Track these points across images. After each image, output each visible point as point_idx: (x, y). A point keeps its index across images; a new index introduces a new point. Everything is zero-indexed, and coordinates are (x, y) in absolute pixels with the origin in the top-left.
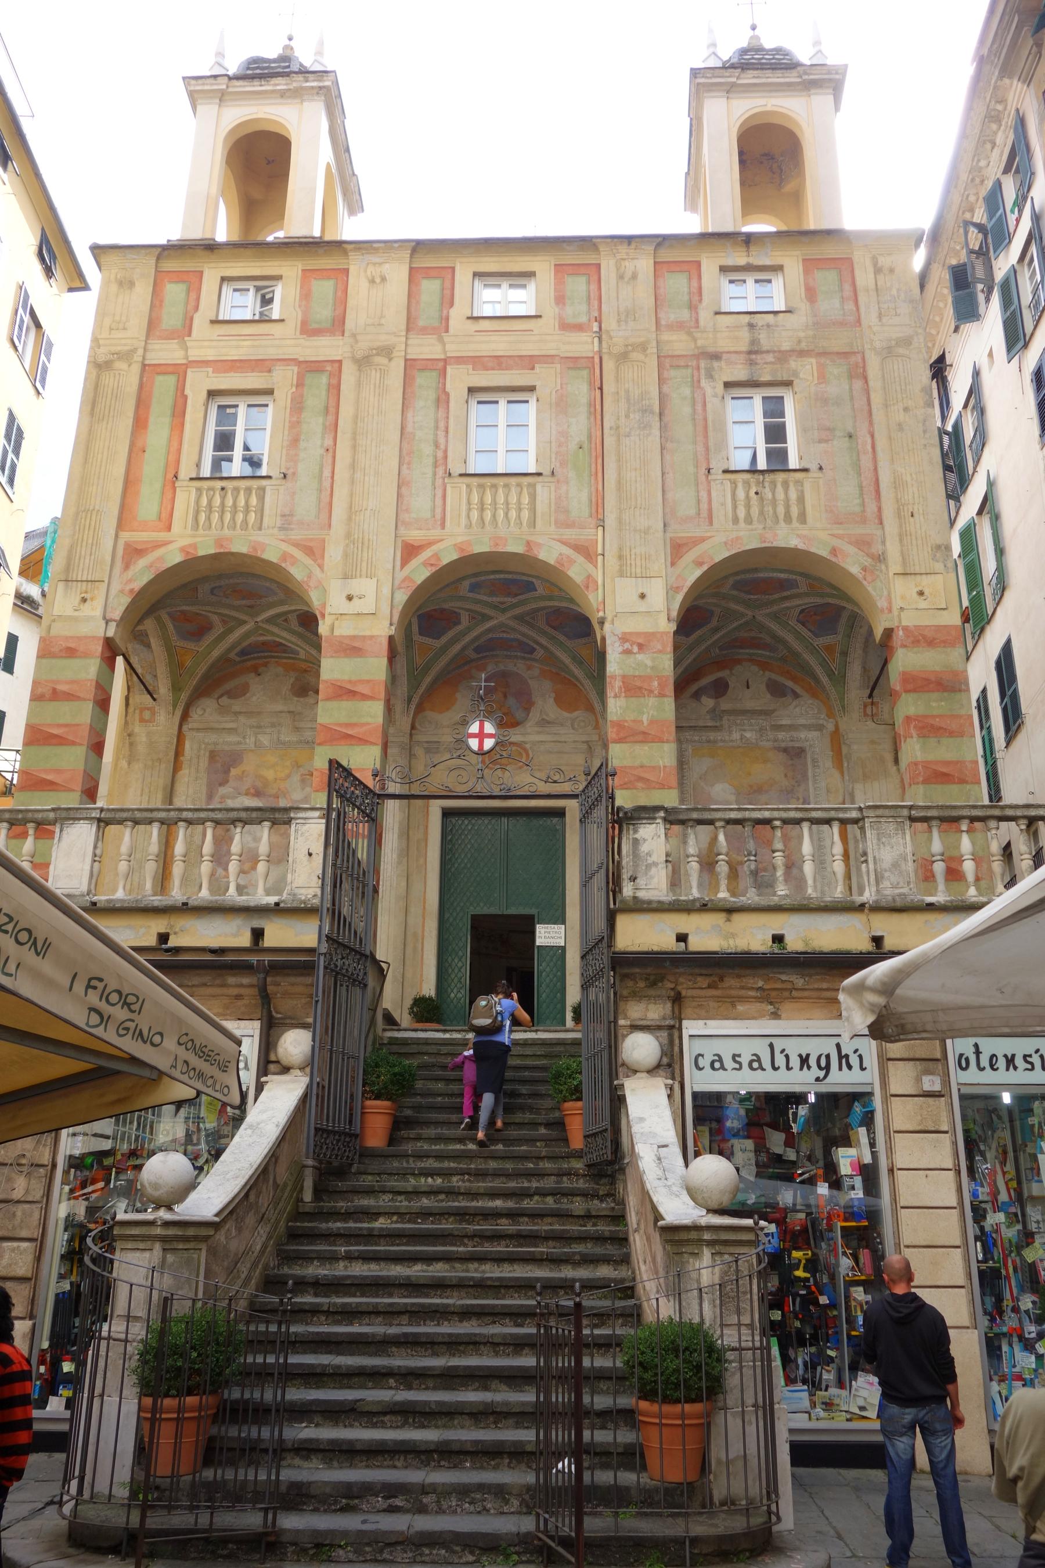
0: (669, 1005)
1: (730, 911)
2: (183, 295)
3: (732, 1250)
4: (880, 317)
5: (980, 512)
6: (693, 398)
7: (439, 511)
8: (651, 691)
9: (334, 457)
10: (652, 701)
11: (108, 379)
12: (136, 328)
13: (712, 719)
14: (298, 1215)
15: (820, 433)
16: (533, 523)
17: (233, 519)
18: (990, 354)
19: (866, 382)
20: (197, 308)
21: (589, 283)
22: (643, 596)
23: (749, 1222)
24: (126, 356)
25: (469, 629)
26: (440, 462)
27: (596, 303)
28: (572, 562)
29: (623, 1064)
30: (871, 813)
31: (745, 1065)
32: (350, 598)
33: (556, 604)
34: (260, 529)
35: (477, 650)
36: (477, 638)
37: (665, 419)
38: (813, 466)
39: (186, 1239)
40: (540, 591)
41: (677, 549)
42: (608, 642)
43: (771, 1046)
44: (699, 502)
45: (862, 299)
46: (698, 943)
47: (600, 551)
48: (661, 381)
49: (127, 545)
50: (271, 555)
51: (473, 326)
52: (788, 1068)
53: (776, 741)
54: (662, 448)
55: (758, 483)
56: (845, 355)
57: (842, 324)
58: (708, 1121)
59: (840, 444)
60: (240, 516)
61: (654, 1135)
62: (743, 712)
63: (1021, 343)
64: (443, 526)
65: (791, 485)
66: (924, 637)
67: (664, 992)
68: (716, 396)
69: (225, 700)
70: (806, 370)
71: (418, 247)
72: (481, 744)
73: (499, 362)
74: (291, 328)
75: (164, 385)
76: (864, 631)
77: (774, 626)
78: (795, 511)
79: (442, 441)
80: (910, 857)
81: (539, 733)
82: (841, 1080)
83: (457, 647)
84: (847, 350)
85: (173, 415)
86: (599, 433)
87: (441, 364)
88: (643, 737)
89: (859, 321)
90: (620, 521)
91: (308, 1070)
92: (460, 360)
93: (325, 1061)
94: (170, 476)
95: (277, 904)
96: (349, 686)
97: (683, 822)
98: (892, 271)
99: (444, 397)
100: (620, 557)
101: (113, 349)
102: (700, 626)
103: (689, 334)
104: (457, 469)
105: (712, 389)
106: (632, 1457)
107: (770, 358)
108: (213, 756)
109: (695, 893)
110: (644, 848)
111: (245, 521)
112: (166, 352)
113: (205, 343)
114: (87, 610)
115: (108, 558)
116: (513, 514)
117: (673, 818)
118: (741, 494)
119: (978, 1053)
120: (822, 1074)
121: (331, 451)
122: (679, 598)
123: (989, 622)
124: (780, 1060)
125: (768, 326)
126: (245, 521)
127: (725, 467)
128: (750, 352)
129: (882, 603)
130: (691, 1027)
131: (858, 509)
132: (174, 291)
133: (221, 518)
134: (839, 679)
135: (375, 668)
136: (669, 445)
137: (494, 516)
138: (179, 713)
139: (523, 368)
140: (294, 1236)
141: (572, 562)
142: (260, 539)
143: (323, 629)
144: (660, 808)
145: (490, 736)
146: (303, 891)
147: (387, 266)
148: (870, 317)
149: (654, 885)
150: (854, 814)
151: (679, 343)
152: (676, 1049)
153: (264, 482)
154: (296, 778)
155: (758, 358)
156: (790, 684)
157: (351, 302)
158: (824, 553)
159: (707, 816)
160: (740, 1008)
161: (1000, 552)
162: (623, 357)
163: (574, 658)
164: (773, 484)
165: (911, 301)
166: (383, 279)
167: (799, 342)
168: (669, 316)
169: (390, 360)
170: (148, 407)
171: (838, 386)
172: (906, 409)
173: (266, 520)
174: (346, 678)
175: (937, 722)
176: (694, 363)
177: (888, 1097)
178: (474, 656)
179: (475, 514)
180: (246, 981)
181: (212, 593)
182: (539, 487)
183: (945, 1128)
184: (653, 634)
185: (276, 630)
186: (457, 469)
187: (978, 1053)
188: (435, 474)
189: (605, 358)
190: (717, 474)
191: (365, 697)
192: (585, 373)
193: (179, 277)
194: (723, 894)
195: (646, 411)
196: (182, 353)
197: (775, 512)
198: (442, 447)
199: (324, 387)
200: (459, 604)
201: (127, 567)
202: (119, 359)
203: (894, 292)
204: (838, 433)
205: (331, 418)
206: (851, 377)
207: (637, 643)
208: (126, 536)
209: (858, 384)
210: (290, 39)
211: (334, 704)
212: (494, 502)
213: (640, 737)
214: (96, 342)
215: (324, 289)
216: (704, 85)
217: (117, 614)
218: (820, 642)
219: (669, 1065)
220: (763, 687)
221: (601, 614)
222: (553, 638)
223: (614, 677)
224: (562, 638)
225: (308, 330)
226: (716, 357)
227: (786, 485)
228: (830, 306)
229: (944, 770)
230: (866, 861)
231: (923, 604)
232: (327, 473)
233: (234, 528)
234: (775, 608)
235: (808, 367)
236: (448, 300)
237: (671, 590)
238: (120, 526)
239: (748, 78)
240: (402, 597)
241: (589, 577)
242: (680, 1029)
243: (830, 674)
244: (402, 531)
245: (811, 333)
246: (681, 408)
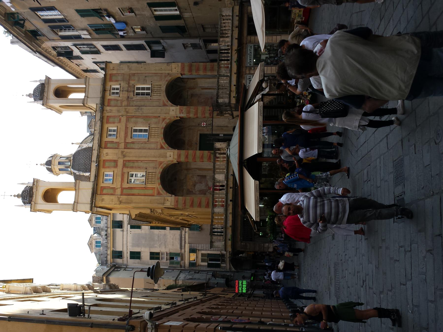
10: (191, 110)
11: (124, 201)
15: (145, 82)
16: (158, 128)
24: (119, 198)
41: (165, 105)
48: (132, 106)
50: (161, 170)
56: (130, 76)
59: (147, 78)
70: (132, 82)
74: (116, 170)
90: (159, 114)
92: (125, 140)
104: (147, 140)
107: (129, 88)
112: (119, 192)
113: (117, 185)
114: (170, 200)
121: (141, 161)
135: (183, 152)
143: (175, 162)
148: (123, 72)
149: (227, 100)
151: (125, 103)
158: (167, 83)
162: (127, 112)
191: (188, 153)
196: (119, 189)
201: (162, 194)
207: (181, 111)
208: (155, 195)
217: (170, 195)
225: (116, 166)
226: (128, 97)
227: (154, 87)
228: (120, 78)
232: (146, 162)
236: (112, 142)
237: (172, 106)
239: (45, 94)
246: (138, 103)
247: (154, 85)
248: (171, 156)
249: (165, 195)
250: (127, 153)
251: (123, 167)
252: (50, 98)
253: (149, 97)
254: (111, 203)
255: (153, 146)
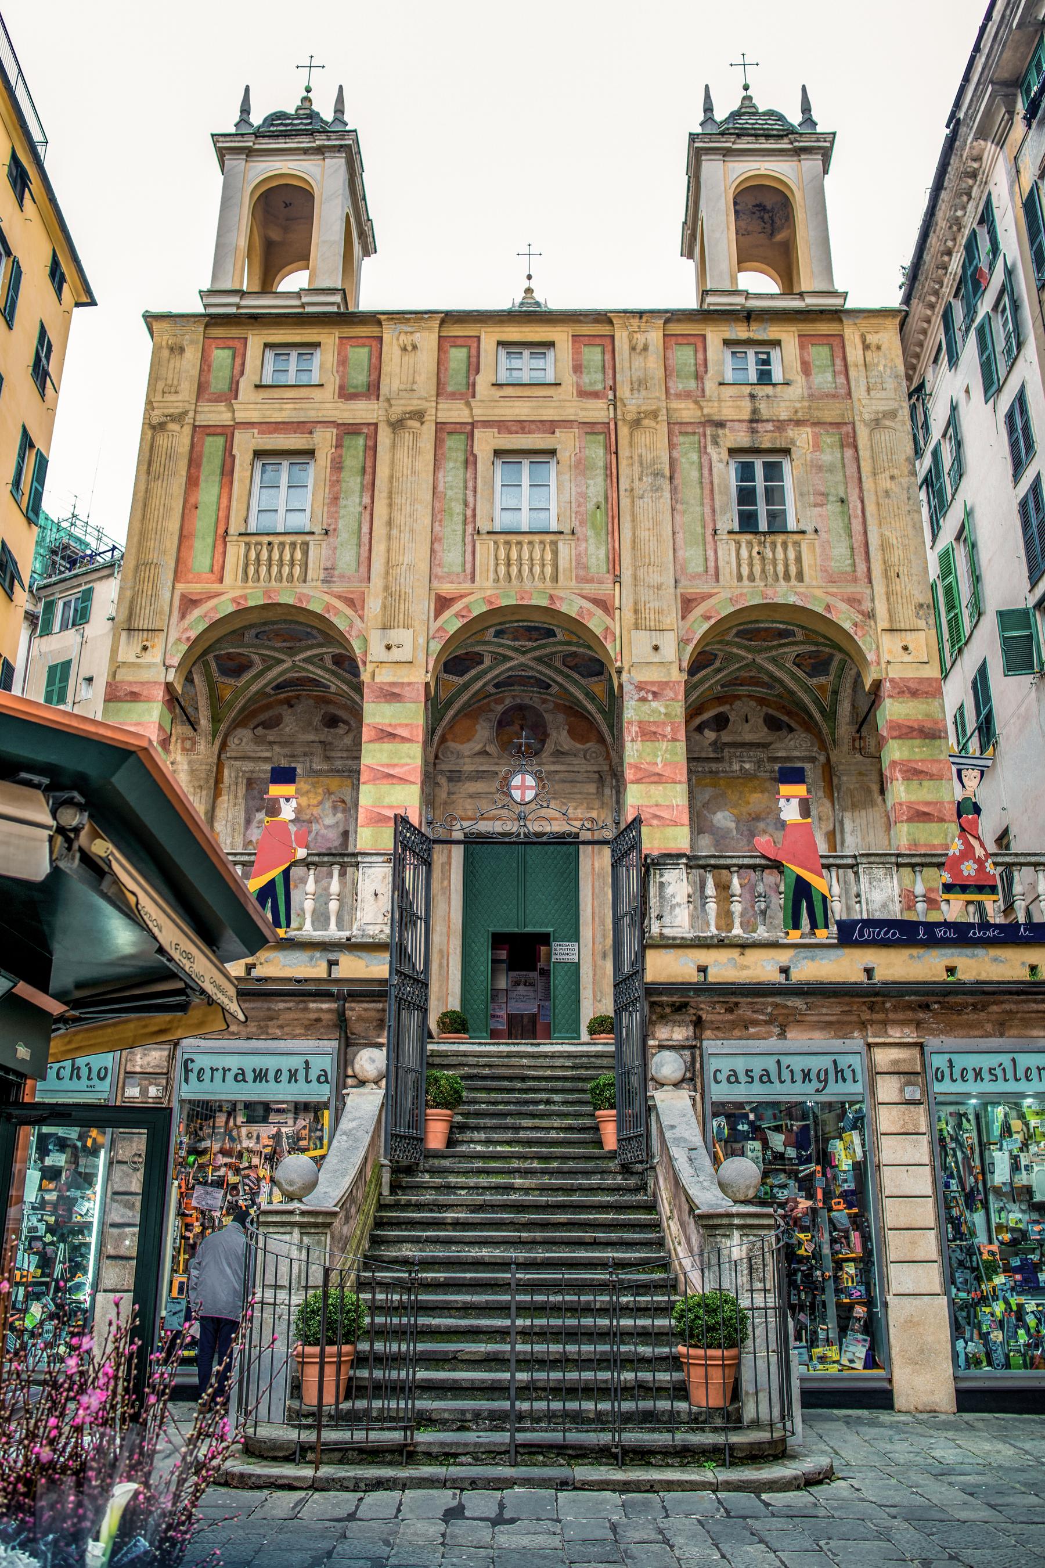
0: (691, 1028)
1: (744, 946)
2: (229, 361)
3: (755, 1232)
4: (868, 390)
5: (958, 539)
6: (701, 463)
7: (469, 566)
8: (665, 736)
9: (372, 515)
10: (664, 745)
11: (162, 440)
12: (187, 391)
13: (714, 751)
14: (382, 1207)
16: (555, 578)
17: (280, 572)
18: (967, 391)
19: (857, 451)
20: (242, 373)
21: (603, 353)
22: (656, 648)
23: (771, 1210)
24: (178, 418)
25: (490, 668)
26: (470, 520)
27: (610, 372)
28: (591, 614)
29: (652, 1079)
30: (864, 860)
31: (756, 1079)
32: (388, 647)
33: (574, 649)
34: (305, 581)
35: (497, 686)
36: (497, 676)
37: (676, 482)
38: (809, 529)
39: (316, 1225)
40: (560, 637)
42: (625, 690)
43: (778, 1062)
44: (706, 560)
45: (852, 373)
46: (714, 975)
47: (617, 605)
48: (671, 446)
49: (183, 596)
51: (498, 393)
52: (793, 1082)
53: (772, 772)
54: (673, 510)
55: (760, 543)
57: (834, 396)
58: (733, 1127)
59: (833, 507)
60: (286, 570)
61: (685, 1140)
62: (743, 745)
63: (995, 388)
64: (473, 580)
65: (790, 545)
66: (908, 688)
67: (688, 1019)
68: (721, 461)
69: (260, 731)
70: (802, 438)
71: (449, 318)
72: (523, 794)
73: (522, 426)
74: (329, 392)
75: (214, 445)
76: (853, 672)
77: (771, 667)
78: (793, 570)
79: (471, 499)
80: (897, 899)
81: (554, 763)
82: (836, 1091)
83: (479, 684)
84: (839, 420)
85: (222, 474)
86: (615, 495)
87: (469, 427)
88: (658, 779)
89: (849, 394)
90: (635, 577)
91: (384, 1083)
92: (487, 424)
93: (393, 1074)
94: (221, 531)
95: (349, 939)
96: (389, 730)
97: (704, 867)
98: (879, 348)
99: (471, 458)
100: (636, 611)
101: (167, 411)
102: (704, 667)
103: (696, 402)
104: (484, 527)
105: (717, 455)
106: (681, 1391)
107: (770, 426)
108: (250, 783)
109: (713, 930)
110: (669, 891)
111: (291, 574)
112: (216, 414)
115: (167, 609)
116: (537, 569)
117: (693, 863)
118: (744, 553)
119: (951, 1066)
120: (821, 1086)
121: (370, 509)
122: (690, 648)
123: (966, 644)
124: (786, 1075)
125: (768, 397)
126: (291, 574)
127: (729, 528)
128: (751, 421)
129: (870, 657)
130: (711, 1045)
131: (849, 569)
132: (221, 356)
133: (269, 571)
134: (831, 716)
136: (678, 507)
137: (520, 571)
138: (218, 743)
139: (544, 432)
140: (379, 1224)
141: (591, 614)
142: (305, 591)
143: (365, 677)
144: (680, 856)
145: (531, 788)
146: (370, 927)
147: (418, 335)
148: (859, 391)
150: (850, 861)
151: (687, 411)
152: (698, 1065)
153: (308, 538)
154: (328, 804)
155: (760, 426)
156: (785, 718)
157: (385, 369)
159: (722, 862)
160: (752, 1030)
161: (976, 579)
162: (636, 424)
163: (587, 694)
164: (774, 545)
165: (896, 377)
166: (415, 347)
167: (796, 412)
168: (678, 386)
169: (422, 423)
170: (199, 466)
171: (829, 456)
172: (892, 478)
173: (310, 572)
174: (387, 721)
175: (920, 766)
176: (701, 430)
177: (876, 1104)
178: (493, 691)
179: (502, 569)
180: (325, 1006)
181: (257, 637)
182: (560, 545)
183: (923, 1130)
184: (667, 683)
185: (311, 668)
186: (484, 527)
187: (951, 1066)
188: (465, 531)
189: (620, 423)
190: (723, 535)
191: (404, 740)
192: (601, 437)
193: (224, 343)
194: (737, 931)
195: (656, 475)
196: (230, 415)
197: (775, 571)
198: (471, 505)
199: (361, 449)
200: (484, 648)
201: (183, 617)
202: (172, 421)
203: (881, 368)
204: (832, 498)
205: (368, 477)
206: (842, 446)
208: (181, 587)
209: (849, 453)
210: (308, 90)
211: (376, 746)
212: (520, 558)
213: (656, 779)
214: (150, 404)
215: (360, 355)
216: (702, 149)
217: (175, 661)
218: (812, 682)
219: (692, 1079)
220: (761, 721)
221: (618, 664)
222: (568, 676)
223: (630, 723)
224: (576, 676)
225: (346, 394)
226: (721, 424)
227: (785, 544)
228: (824, 380)
229: (926, 810)
230: (859, 902)
231: (907, 658)
232: (365, 529)
233: (281, 581)
234: (774, 653)
235: (804, 436)
236: (474, 367)
237: (683, 642)
238: (176, 579)
239: (742, 144)
240: (436, 646)
241: (607, 628)
242: (701, 1048)
243: (822, 711)
244: (435, 584)
245: (806, 404)
247: (797, 544)
248: (398, 658)
249: (173, 635)
250: (416, 436)
251: (338, 425)
252: (731, 165)
253: (729, 520)
254: (160, 385)
255: (452, 557)
